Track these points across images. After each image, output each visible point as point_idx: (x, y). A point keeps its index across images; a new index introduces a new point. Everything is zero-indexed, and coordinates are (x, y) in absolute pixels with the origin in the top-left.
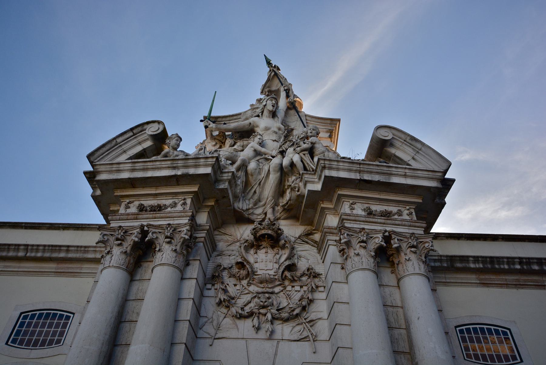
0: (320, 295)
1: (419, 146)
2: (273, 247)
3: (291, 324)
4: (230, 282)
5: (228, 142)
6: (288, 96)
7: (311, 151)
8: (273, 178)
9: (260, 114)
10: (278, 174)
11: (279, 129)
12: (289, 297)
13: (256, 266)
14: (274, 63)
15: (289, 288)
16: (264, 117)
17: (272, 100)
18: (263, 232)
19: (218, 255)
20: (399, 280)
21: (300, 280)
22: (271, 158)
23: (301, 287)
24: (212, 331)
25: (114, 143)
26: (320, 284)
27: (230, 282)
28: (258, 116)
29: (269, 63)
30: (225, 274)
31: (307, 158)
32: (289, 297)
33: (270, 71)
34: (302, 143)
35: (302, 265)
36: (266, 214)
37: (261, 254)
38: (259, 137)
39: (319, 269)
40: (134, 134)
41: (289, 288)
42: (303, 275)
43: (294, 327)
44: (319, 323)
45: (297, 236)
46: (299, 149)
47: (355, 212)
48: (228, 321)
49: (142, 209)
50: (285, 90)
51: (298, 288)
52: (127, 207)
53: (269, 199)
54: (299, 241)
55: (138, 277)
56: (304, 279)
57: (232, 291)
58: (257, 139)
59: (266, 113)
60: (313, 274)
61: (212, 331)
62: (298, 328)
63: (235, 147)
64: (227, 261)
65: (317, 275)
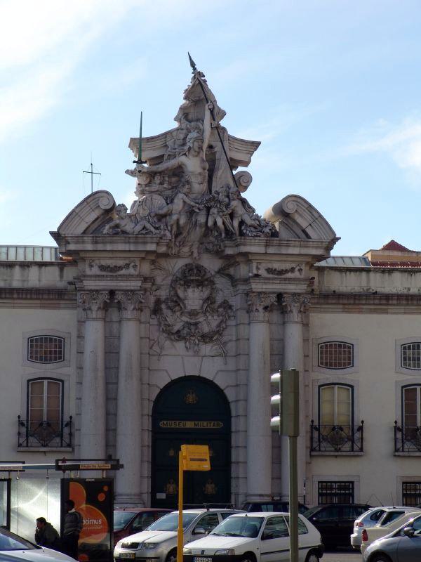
0: (231, 323)
1: (316, 215)
2: (198, 286)
3: (211, 344)
4: (166, 312)
5: (157, 179)
6: (213, 117)
7: (232, 216)
8: (198, 232)
9: (187, 153)
10: (204, 229)
11: (204, 169)
12: (209, 324)
13: (186, 302)
14: (199, 68)
15: (210, 317)
16: (190, 157)
17: (198, 142)
18: (192, 278)
19: (157, 290)
20: (284, 323)
21: (217, 311)
22: (197, 210)
23: (218, 316)
24: (158, 351)
25: (74, 214)
26: (232, 314)
27: (166, 312)
28: (185, 154)
29: (193, 64)
30: (163, 306)
31: (228, 222)
32: (209, 324)
33: (194, 77)
34: (224, 209)
35: (219, 299)
36: (192, 252)
37: (190, 291)
38: (187, 186)
39: (232, 301)
40: (88, 204)
41: (210, 317)
42: (220, 306)
43: (212, 347)
44: (229, 345)
45: (216, 270)
46: (221, 214)
47: (260, 272)
48: (168, 343)
49: (102, 268)
50: (210, 109)
51: (216, 317)
52: (91, 266)
53: (196, 243)
54: (218, 276)
55: (107, 319)
56: (220, 310)
57: (170, 320)
58: (186, 189)
59: (192, 151)
60: (226, 306)
61: (158, 351)
62: (214, 348)
63: (165, 185)
64: (163, 294)
65: (230, 307)
